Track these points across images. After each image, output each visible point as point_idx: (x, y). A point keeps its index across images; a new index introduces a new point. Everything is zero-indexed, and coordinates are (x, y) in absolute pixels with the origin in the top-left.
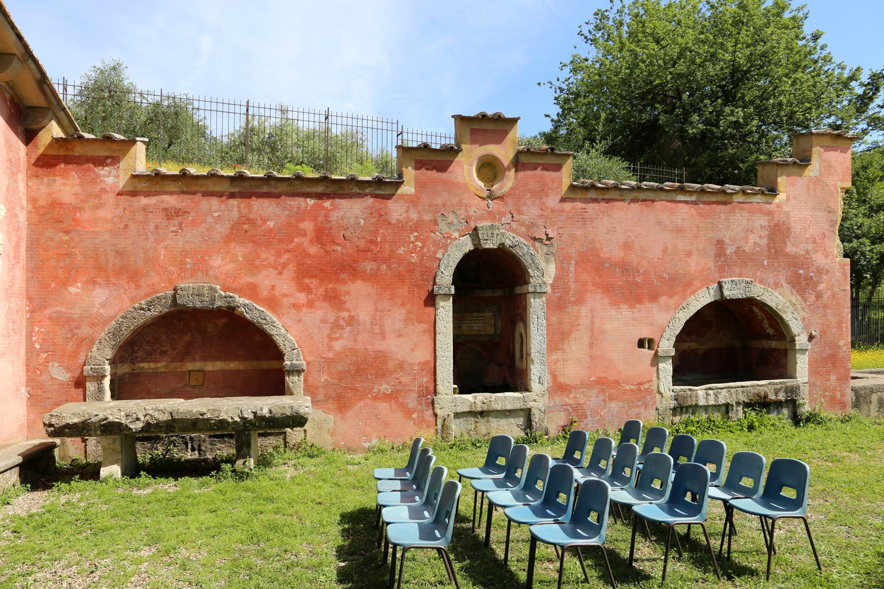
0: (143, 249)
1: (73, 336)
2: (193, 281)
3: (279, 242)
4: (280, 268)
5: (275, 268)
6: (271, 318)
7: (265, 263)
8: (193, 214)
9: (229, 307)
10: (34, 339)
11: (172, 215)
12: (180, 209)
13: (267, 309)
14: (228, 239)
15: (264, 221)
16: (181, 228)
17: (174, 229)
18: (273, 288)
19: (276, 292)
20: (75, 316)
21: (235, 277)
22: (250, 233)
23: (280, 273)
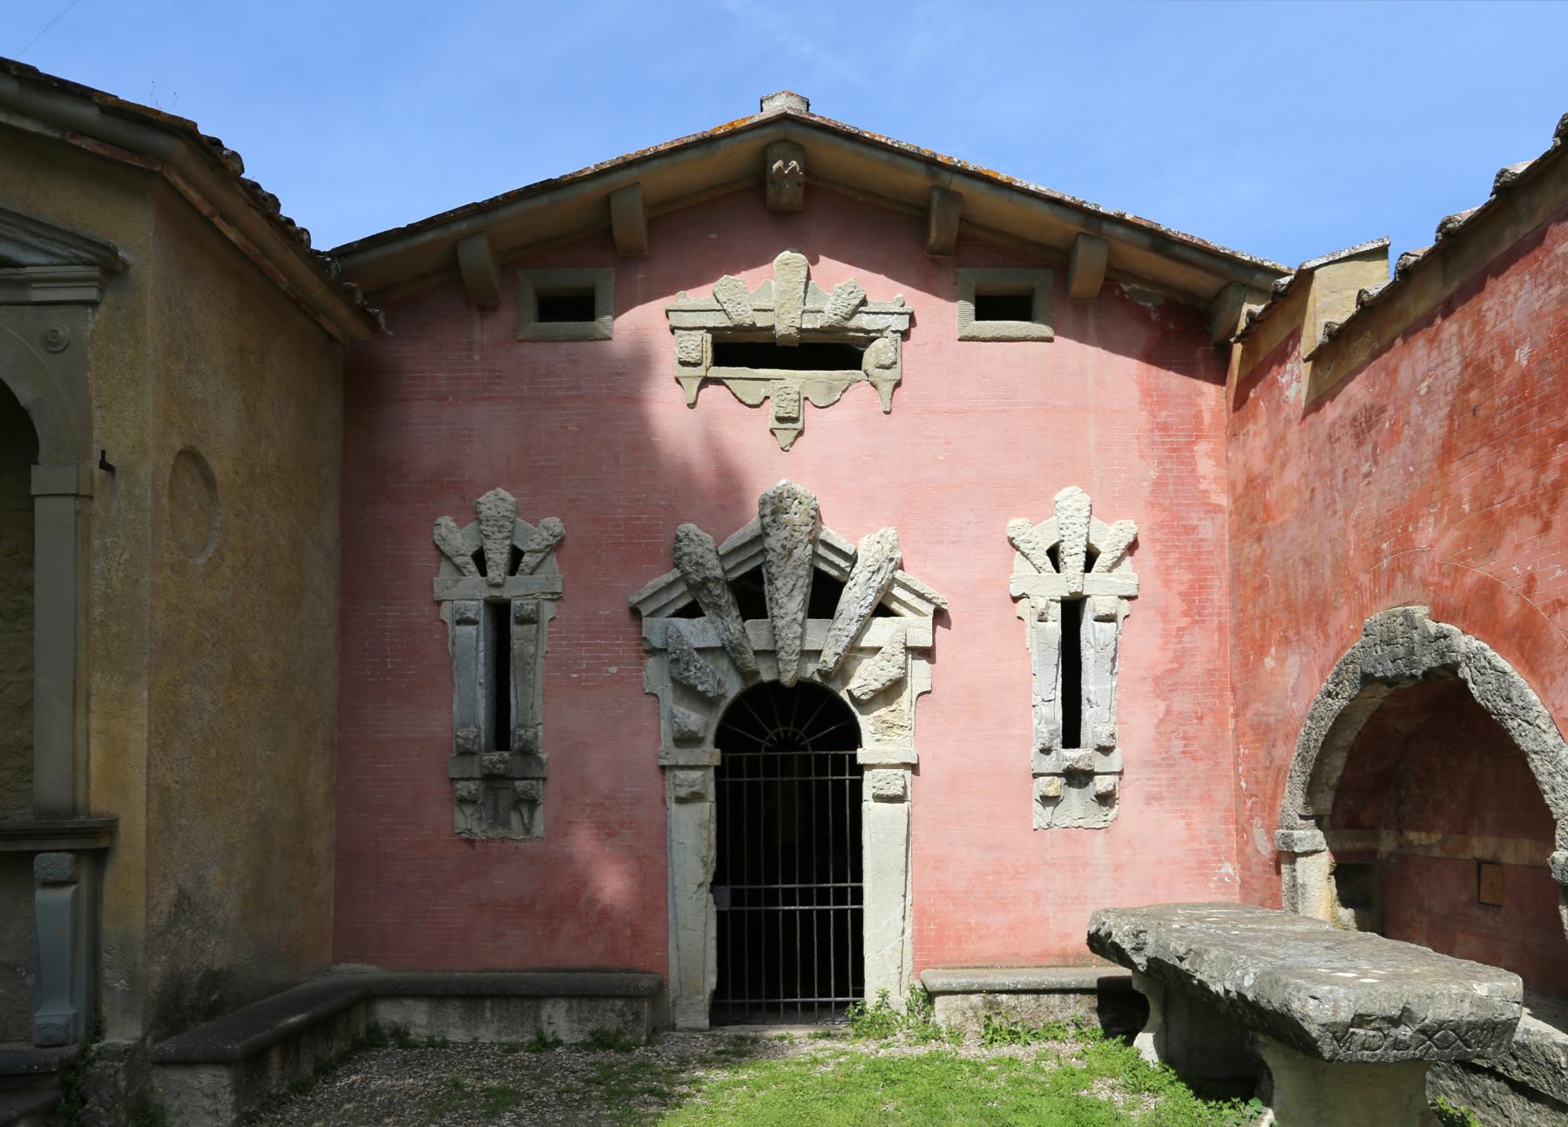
0: (1331, 541)
1: (1271, 762)
2: (1390, 603)
3: (1541, 411)
4: (1544, 508)
5: (1534, 511)
6: (1522, 695)
7: (1513, 502)
8: (1390, 411)
9: (1444, 667)
10: (1240, 769)
11: (1363, 430)
12: (1372, 407)
13: (1516, 663)
14: (1447, 453)
15: (1508, 353)
16: (1376, 463)
17: (1365, 469)
18: (1531, 580)
19: (1538, 603)
20: (1272, 719)
21: (1456, 569)
22: (1482, 413)
23: (1546, 527)
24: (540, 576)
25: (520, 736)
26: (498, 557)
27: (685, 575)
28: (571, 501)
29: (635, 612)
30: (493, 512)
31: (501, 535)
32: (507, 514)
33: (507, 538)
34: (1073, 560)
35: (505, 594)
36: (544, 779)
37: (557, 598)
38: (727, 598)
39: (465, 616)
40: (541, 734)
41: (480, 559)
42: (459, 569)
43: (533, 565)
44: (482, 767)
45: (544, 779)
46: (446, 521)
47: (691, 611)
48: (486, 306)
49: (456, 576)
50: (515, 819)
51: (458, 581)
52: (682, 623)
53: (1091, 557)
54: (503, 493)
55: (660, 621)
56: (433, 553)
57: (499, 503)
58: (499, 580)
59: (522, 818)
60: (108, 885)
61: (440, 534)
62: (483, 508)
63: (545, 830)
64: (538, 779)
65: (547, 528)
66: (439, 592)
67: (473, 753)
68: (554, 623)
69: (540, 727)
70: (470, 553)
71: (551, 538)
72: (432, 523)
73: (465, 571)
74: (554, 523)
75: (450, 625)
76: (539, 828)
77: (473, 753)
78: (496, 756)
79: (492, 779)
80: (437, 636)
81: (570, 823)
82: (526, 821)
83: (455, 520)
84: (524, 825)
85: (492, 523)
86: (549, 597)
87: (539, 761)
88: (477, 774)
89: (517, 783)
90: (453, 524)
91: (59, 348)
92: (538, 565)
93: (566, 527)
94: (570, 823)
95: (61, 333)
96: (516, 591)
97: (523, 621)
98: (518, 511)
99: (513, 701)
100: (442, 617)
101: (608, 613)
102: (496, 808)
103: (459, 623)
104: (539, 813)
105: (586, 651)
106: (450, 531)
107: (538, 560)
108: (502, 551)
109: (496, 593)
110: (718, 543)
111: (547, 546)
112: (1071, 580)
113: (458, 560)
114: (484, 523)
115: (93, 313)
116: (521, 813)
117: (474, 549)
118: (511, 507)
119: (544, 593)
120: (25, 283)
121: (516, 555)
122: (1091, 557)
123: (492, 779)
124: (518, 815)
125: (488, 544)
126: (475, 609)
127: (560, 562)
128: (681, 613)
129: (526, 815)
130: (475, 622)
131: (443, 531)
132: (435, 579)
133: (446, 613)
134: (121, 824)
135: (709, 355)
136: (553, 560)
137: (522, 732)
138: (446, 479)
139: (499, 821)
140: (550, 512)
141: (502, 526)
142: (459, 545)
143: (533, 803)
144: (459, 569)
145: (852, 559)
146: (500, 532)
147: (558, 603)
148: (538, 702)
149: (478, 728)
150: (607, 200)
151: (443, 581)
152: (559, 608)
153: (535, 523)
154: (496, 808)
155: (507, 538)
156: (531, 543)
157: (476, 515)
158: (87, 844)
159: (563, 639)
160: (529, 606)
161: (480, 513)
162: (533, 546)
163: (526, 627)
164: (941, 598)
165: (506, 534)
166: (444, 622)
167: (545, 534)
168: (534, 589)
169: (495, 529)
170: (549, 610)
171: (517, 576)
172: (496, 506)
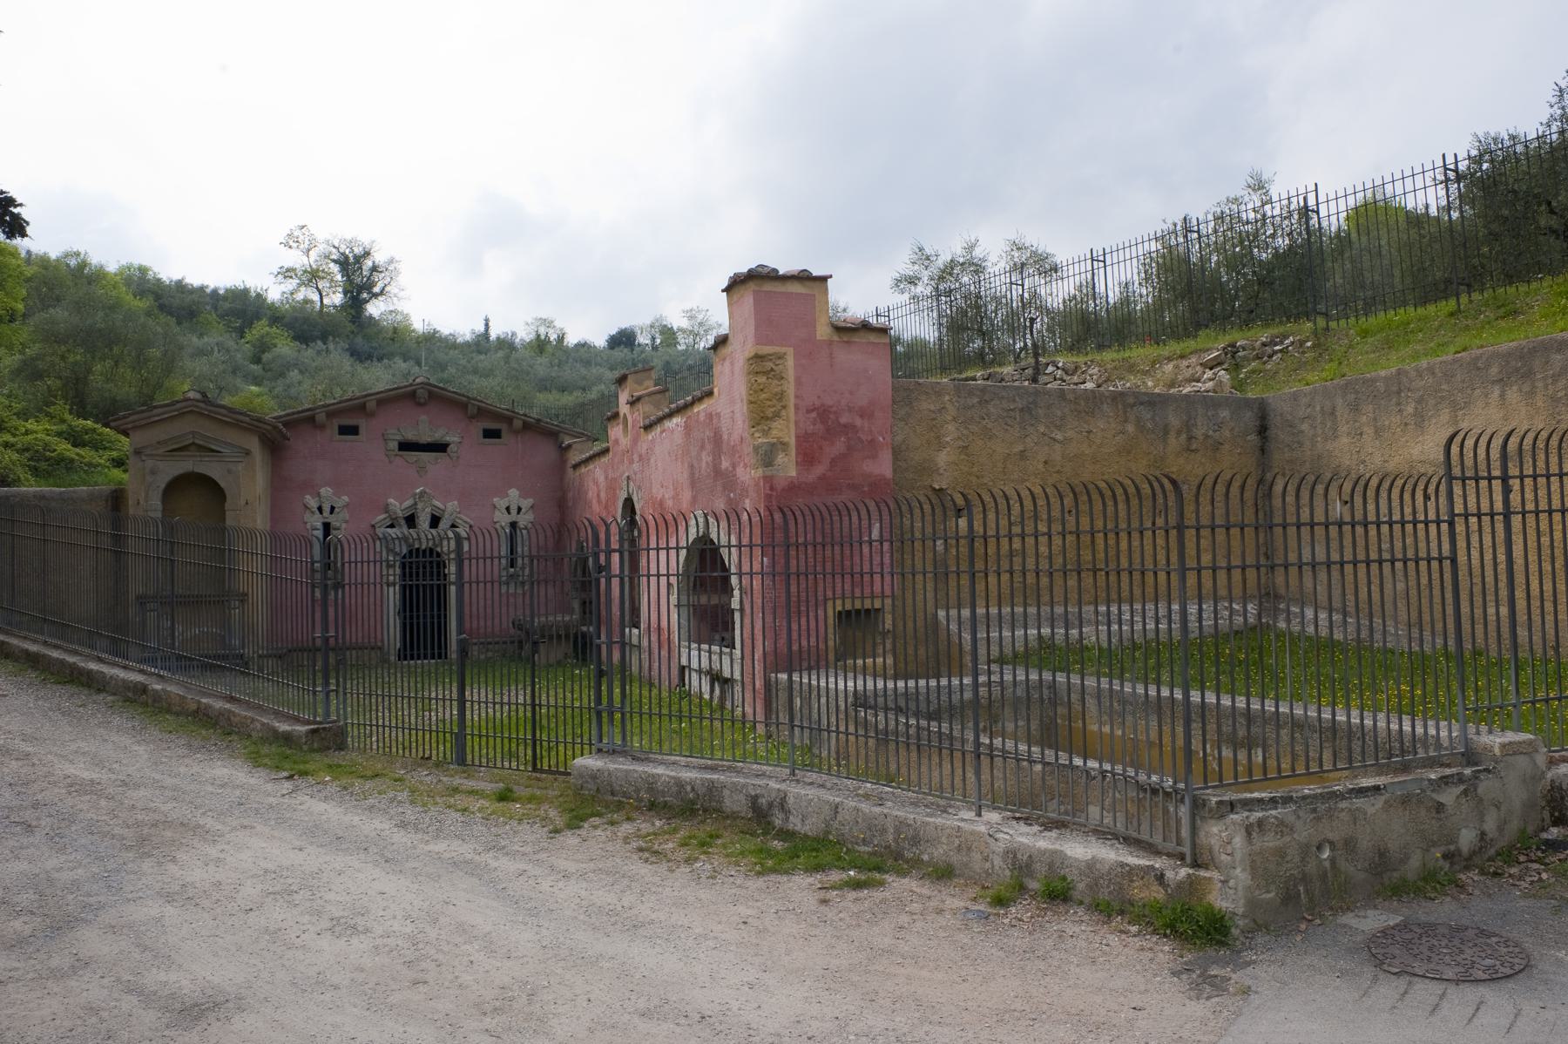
24: (341, 515)
26: (327, 509)
27: (390, 516)
29: (373, 526)
34: (514, 511)
37: (346, 522)
38: (403, 522)
41: (320, 509)
42: (313, 513)
46: (308, 497)
47: (392, 526)
48: (322, 427)
52: (389, 530)
53: (519, 509)
55: (382, 529)
66: (306, 520)
74: (346, 498)
96: (333, 520)
97: (335, 529)
98: (334, 494)
109: (326, 520)
110: (401, 504)
112: (514, 517)
121: (333, 509)
122: (519, 509)
125: (323, 505)
126: (319, 525)
128: (388, 527)
133: (308, 526)
135: (397, 447)
144: (313, 513)
145: (444, 511)
150: (365, 403)
151: (307, 517)
157: (319, 495)
160: (338, 524)
164: (472, 523)
170: (344, 526)
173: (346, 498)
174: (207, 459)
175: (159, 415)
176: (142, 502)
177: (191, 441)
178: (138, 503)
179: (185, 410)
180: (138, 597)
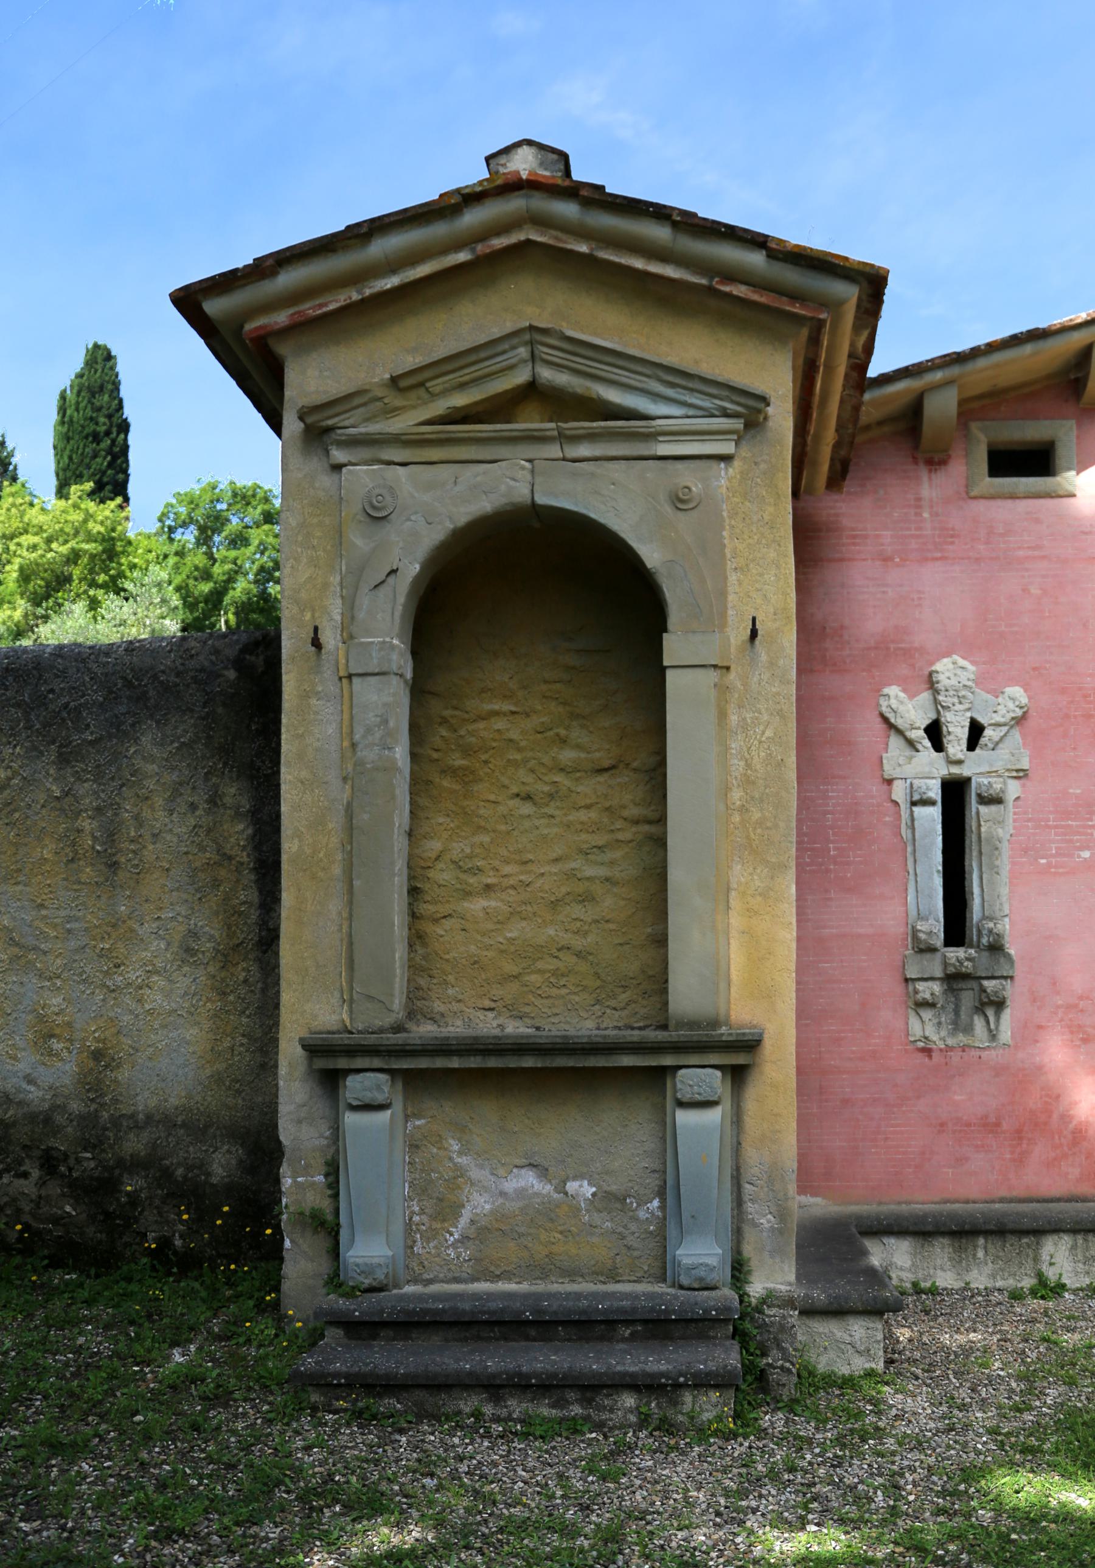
24: (1003, 752)
25: (990, 931)
26: (957, 732)
28: (1035, 669)
30: (954, 682)
31: (961, 707)
32: (970, 683)
33: (969, 709)
35: (965, 771)
36: (1012, 978)
39: (925, 797)
40: (1007, 927)
41: (935, 733)
42: (911, 744)
43: (996, 739)
44: (945, 964)
45: (1012, 978)
46: (893, 691)
49: (908, 752)
50: (979, 1023)
51: (911, 758)
54: (962, 662)
56: (879, 726)
57: (959, 672)
58: (960, 756)
59: (988, 1022)
60: (750, 1105)
61: (890, 706)
62: (941, 677)
63: (1013, 1037)
64: (1005, 978)
65: (1013, 699)
66: (889, 770)
67: (932, 950)
68: (1019, 803)
69: (1007, 920)
70: (923, 727)
71: (1017, 709)
72: (878, 692)
73: (919, 747)
75: (903, 806)
76: (1006, 1033)
77: (932, 950)
78: (960, 953)
79: (954, 979)
80: (887, 819)
81: (1040, 1027)
82: (992, 1026)
83: (904, 691)
84: (990, 1030)
85: (951, 693)
86: (1015, 774)
87: (1008, 957)
88: (938, 973)
89: (986, 983)
90: (902, 695)
91: (691, 506)
92: (1002, 739)
93: (1030, 698)
94: (1040, 1027)
95: (694, 489)
97: (984, 800)
99: (976, 890)
100: (894, 797)
101: (1078, 791)
102: (957, 1012)
103: (914, 804)
104: (1006, 1015)
105: (1056, 834)
106: (902, 703)
107: (1002, 734)
108: (963, 723)
109: (955, 770)
111: (1013, 719)
113: (914, 735)
114: (942, 693)
115: (726, 468)
116: (986, 1016)
117: (927, 722)
118: (972, 677)
119: (1008, 770)
120: (652, 436)
121: (976, 731)
123: (954, 979)
124: (982, 1020)
125: (947, 717)
127: (1024, 736)
129: (992, 1019)
130: (931, 803)
131: (894, 703)
132: (884, 755)
133: (899, 792)
134: (766, 1036)
136: (1016, 734)
137: (991, 925)
138: (892, 646)
139: (959, 1026)
140: (1013, 681)
141: (964, 697)
142: (913, 717)
143: (999, 1005)
144: (911, 744)
146: (960, 703)
147: (1022, 781)
148: (1004, 891)
149: (938, 921)
152: (1023, 786)
153: (997, 693)
154: (957, 1012)
155: (969, 709)
156: (994, 715)
157: (931, 684)
158: (740, 1059)
159: (1029, 820)
161: (938, 682)
162: (998, 718)
163: (993, 808)
165: (967, 706)
166: (896, 803)
167: (1011, 705)
168: (999, 766)
169: (956, 700)
170: (1013, 789)
171: (978, 751)
172: (955, 675)
173: (1017, 692)
174: (584, 450)
175: (392, 266)
176: (330, 639)
177: (521, 377)
178: (316, 643)
179: (500, 242)
180: (314, 1049)
